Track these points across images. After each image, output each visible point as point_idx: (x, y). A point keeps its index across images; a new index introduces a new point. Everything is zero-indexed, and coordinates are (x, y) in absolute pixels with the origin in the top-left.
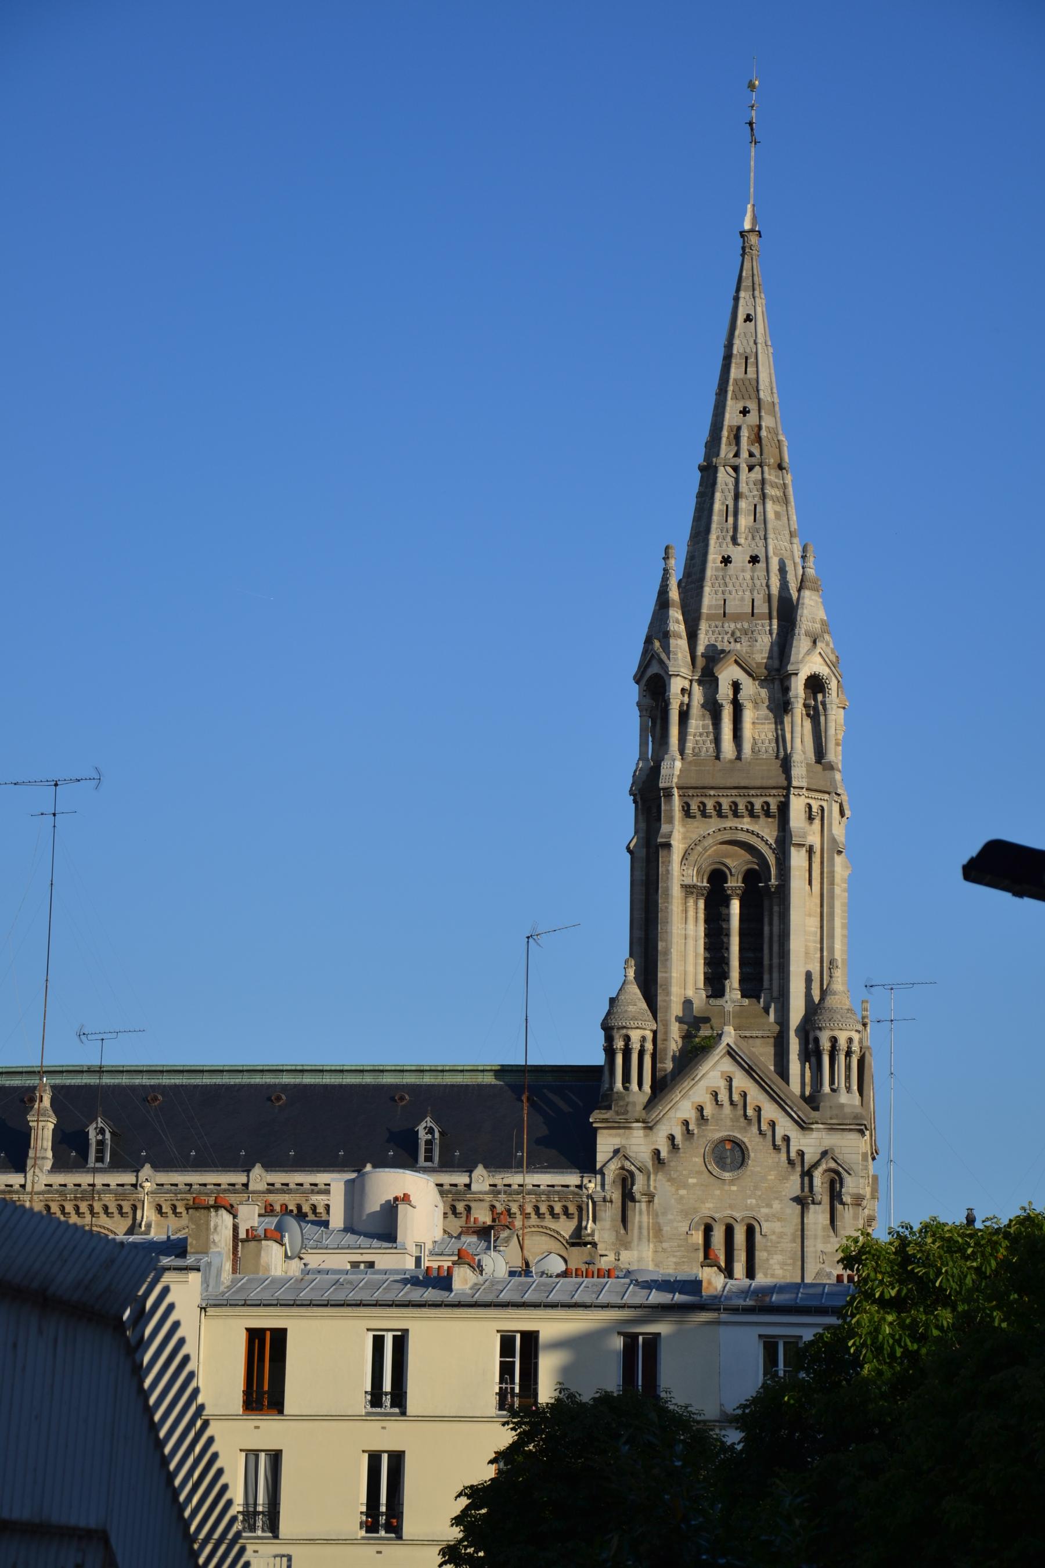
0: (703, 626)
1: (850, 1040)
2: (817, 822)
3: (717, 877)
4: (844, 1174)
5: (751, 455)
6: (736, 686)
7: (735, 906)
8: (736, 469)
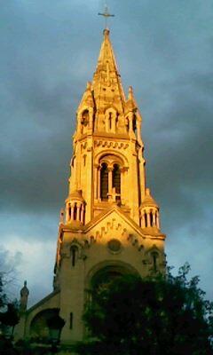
7: (110, 174)
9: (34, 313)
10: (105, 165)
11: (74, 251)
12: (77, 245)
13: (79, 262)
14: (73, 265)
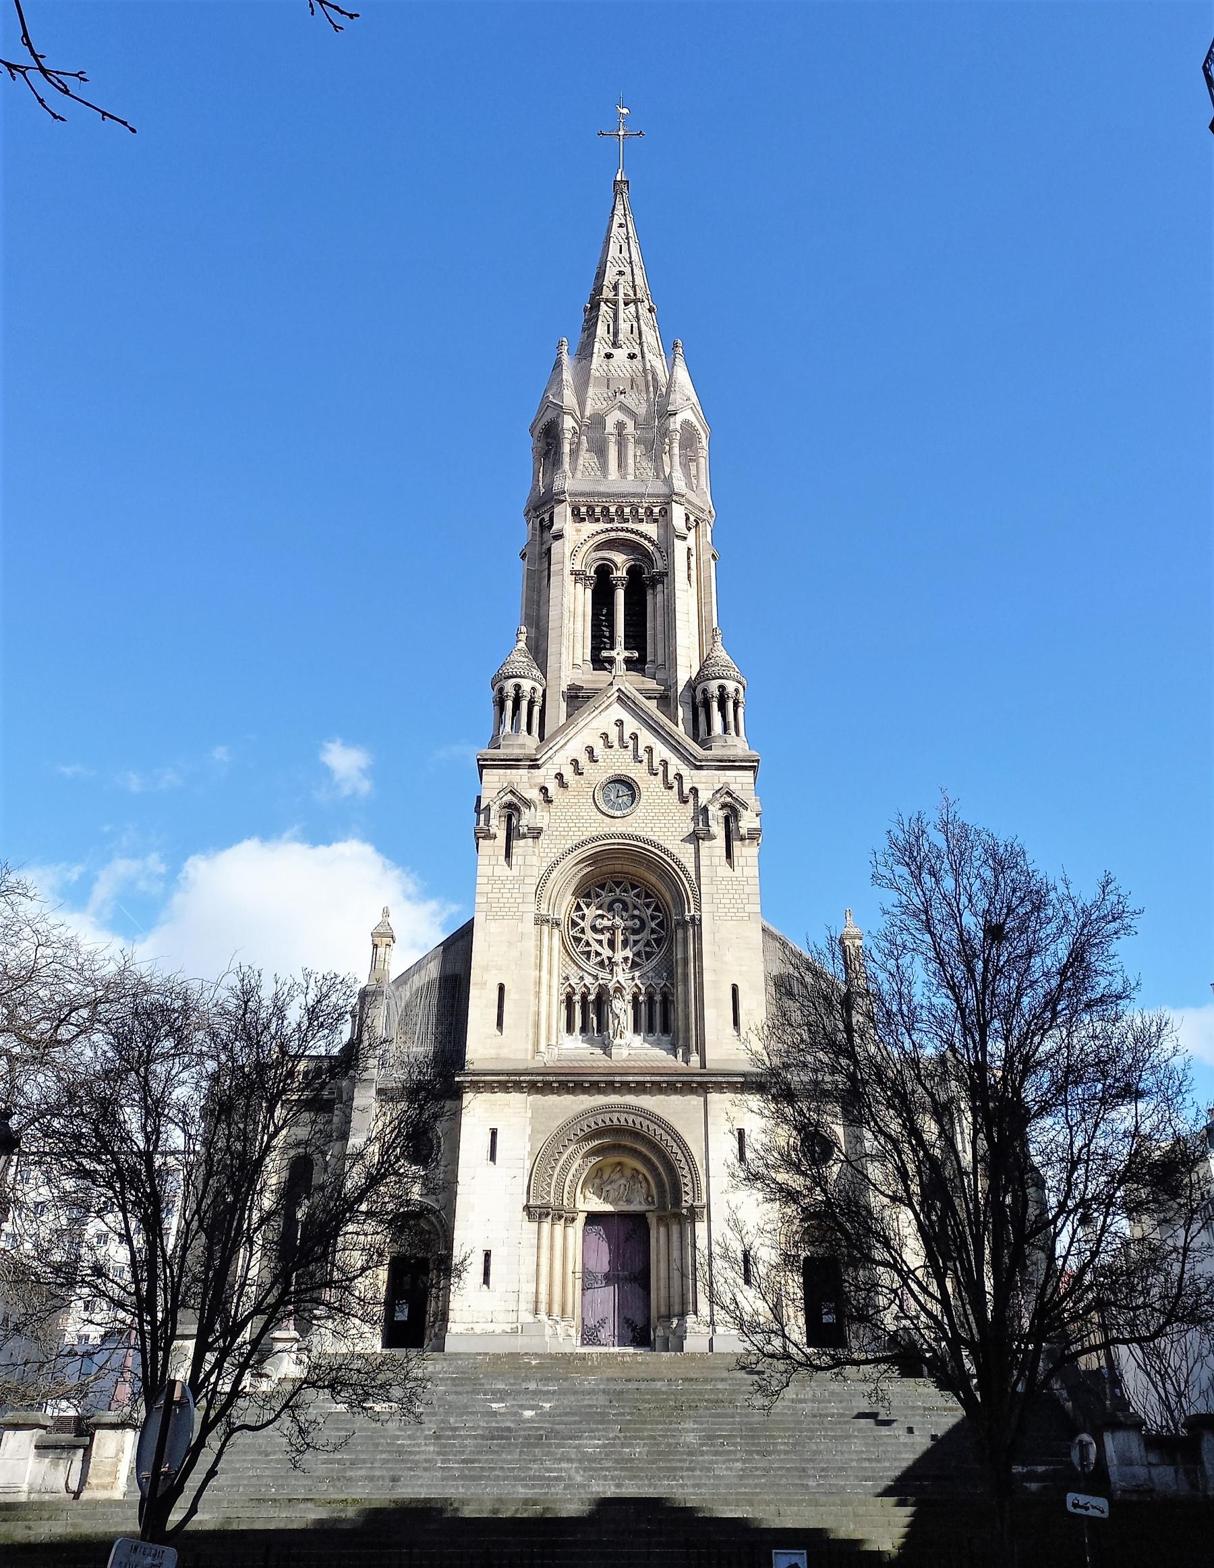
0: (591, 391)
1: (737, 690)
2: (693, 530)
3: (604, 571)
4: (741, 809)
5: (625, 295)
6: (620, 426)
7: (620, 595)
8: (615, 303)
9: (406, 993)
10: (604, 571)
11: (509, 818)
12: (515, 800)
13: (519, 846)
14: (508, 854)
